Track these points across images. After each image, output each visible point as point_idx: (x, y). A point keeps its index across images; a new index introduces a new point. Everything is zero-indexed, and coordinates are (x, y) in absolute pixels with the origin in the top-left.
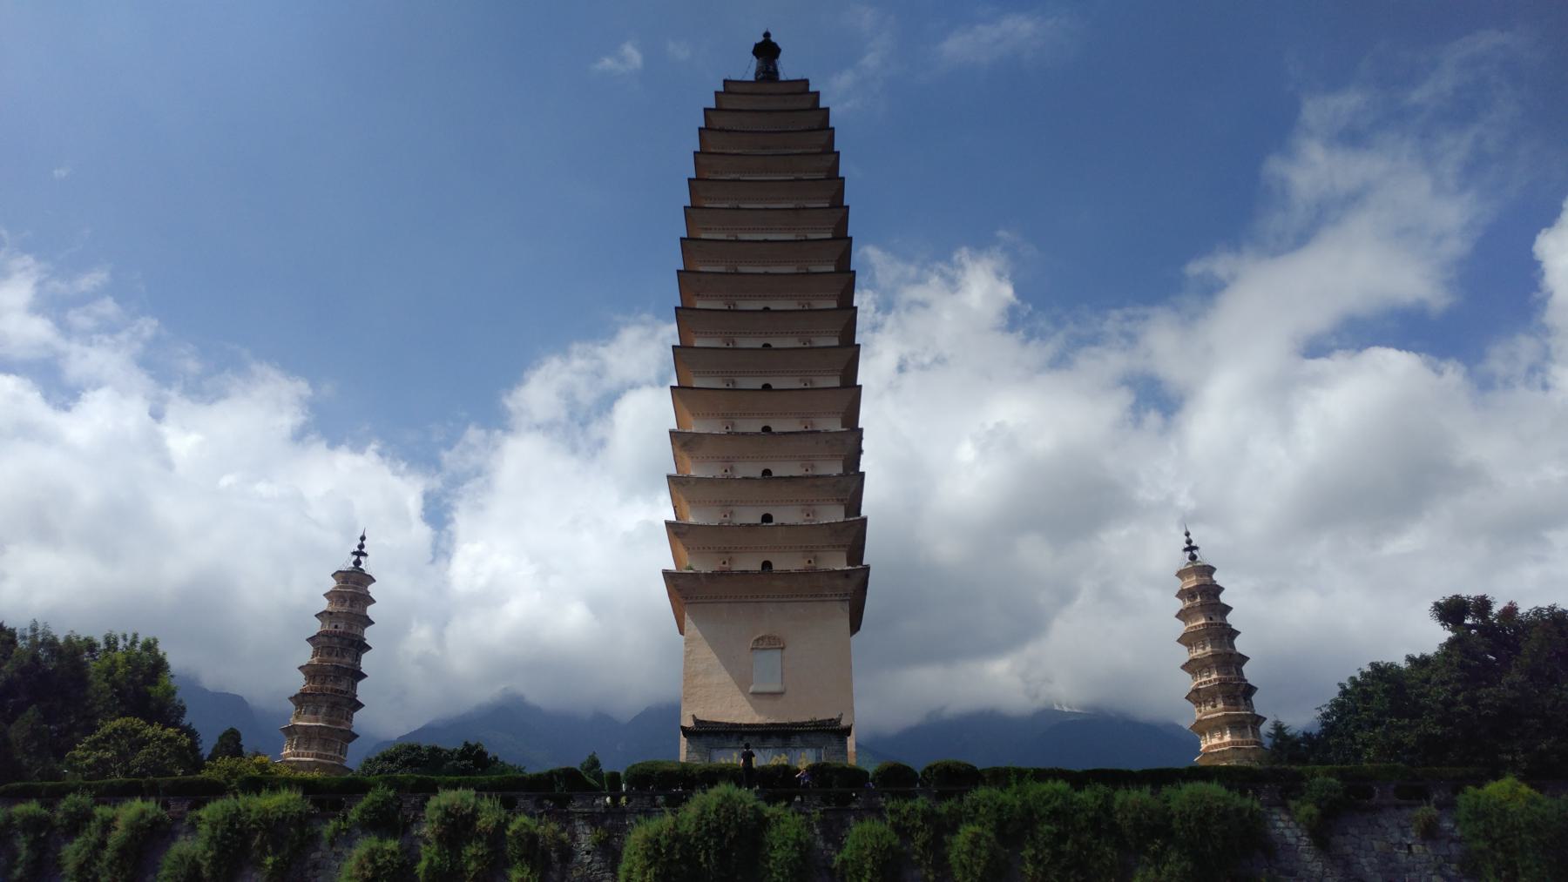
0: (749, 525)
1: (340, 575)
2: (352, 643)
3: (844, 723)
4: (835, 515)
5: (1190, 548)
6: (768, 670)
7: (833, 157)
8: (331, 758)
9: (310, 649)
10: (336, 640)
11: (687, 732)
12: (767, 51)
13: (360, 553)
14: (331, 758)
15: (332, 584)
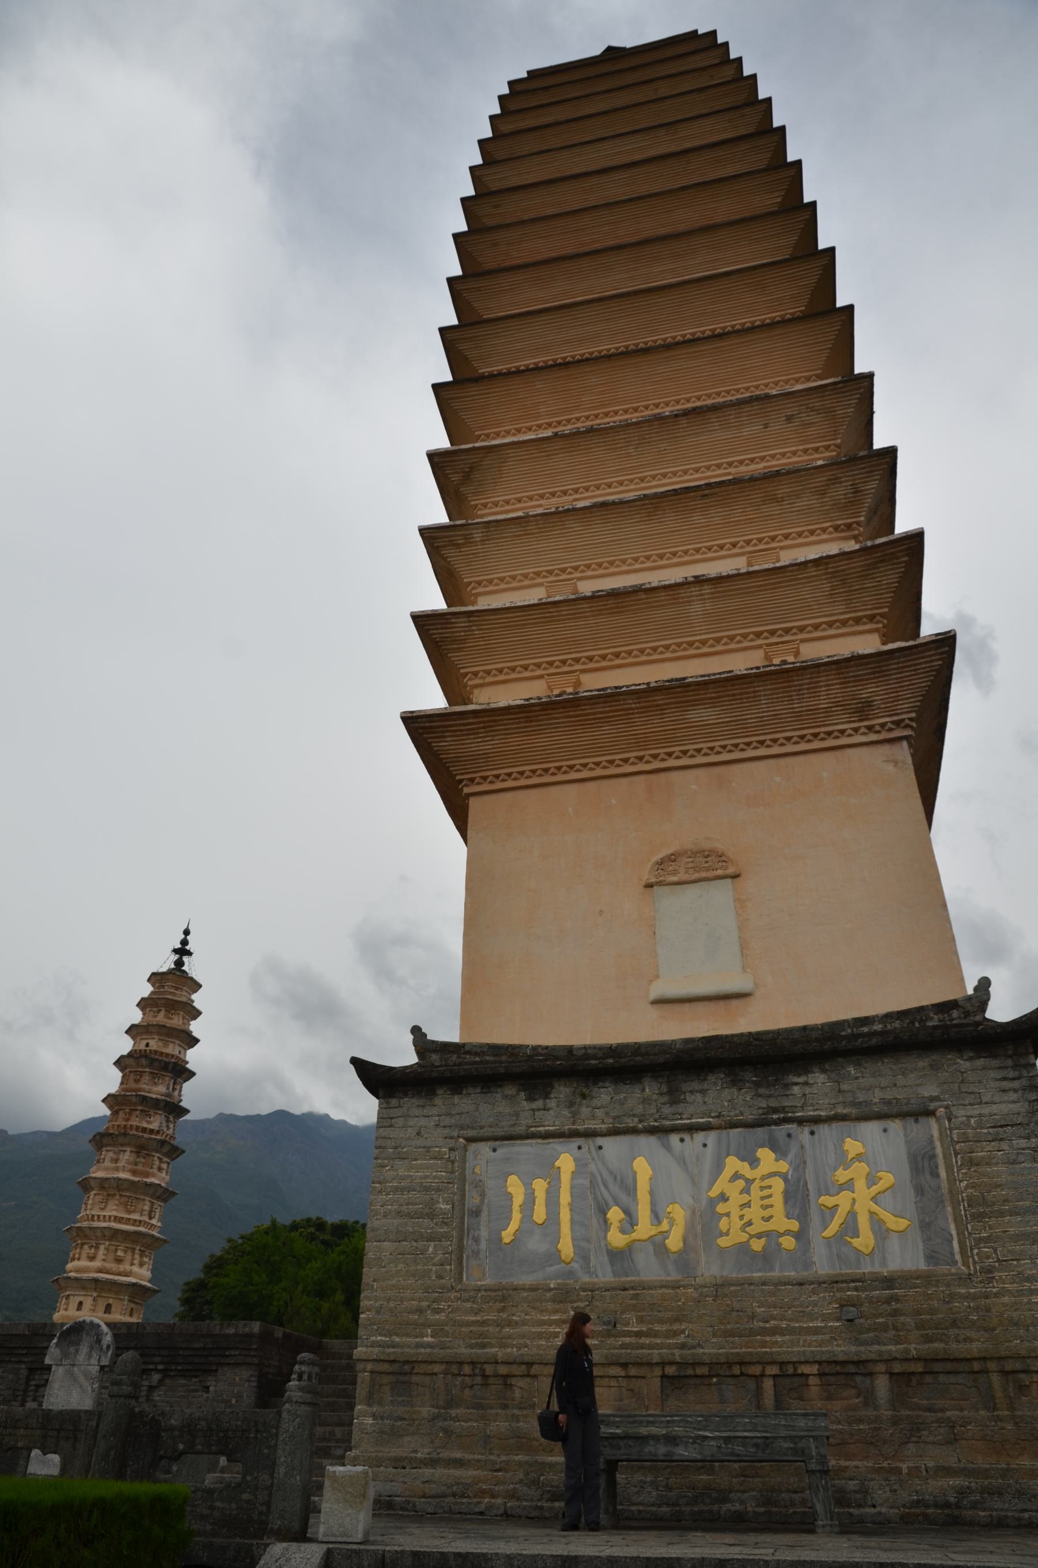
1: (155, 978)
8: (136, 1222)
9: (117, 1075)
10: (144, 1061)
13: (183, 951)
14: (136, 1222)
15: (146, 990)
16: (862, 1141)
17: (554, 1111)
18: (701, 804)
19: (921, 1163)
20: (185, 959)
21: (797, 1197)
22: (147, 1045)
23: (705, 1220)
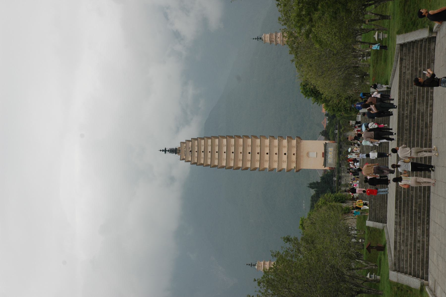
0: (288, 157)
4: (285, 142)
5: (258, 38)
6: (313, 155)
12: (165, 151)
17: (327, 160)
18: (304, 153)
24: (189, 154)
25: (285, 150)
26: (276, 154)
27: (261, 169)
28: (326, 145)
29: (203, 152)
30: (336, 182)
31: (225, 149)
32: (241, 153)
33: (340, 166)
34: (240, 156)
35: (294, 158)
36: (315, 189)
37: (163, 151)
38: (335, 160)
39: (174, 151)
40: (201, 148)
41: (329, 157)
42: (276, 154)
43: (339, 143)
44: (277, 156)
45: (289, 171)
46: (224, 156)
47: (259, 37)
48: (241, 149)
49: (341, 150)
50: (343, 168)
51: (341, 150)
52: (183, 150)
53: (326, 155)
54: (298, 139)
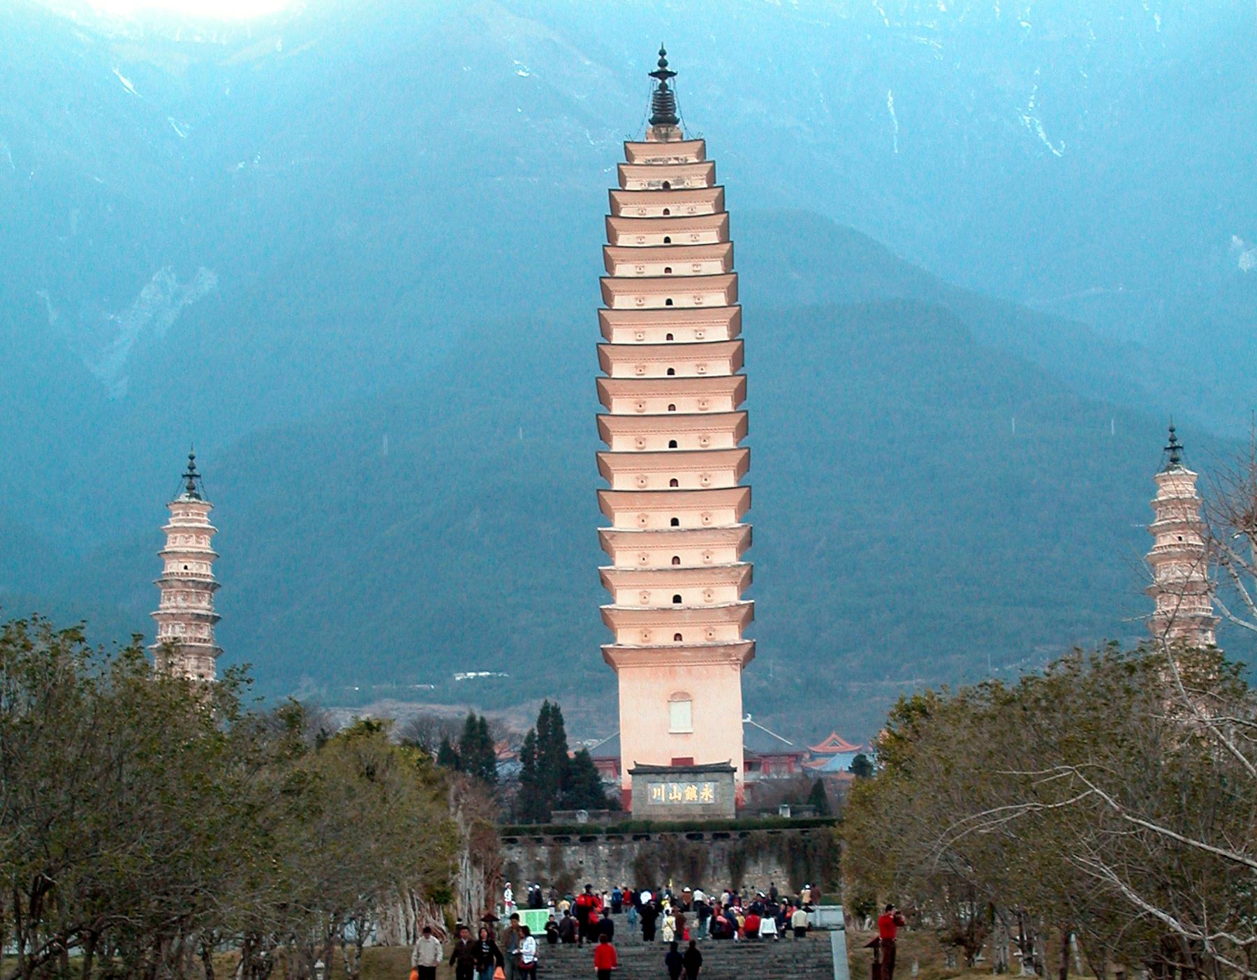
2: (206, 586)
3: (732, 765)
6: (680, 716)
7: (727, 246)
11: (630, 772)
12: (663, 74)
16: (707, 785)
18: (683, 679)
19: (716, 789)
20: (194, 480)
21: (698, 793)
22: (186, 568)
23: (684, 795)
24: (658, 177)
25: (693, 597)
26: (676, 560)
27: (606, 496)
28: (725, 769)
29: (667, 240)
30: (570, 823)
31: (683, 335)
32: (672, 407)
33: (636, 838)
34: (657, 406)
35: (663, 637)
36: (537, 733)
37: (663, 63)
38: (662, 812)
39: (664, 113)
40: (685, 229)
41: (675, 787)
42: (676, 560)
43: (733, 826)
44: (668, 564)
45: (605, 618)
46: (656, 336)
47: (1179, 453)
48: (686, 405)
49: (707, 836)
50: (632, 849)
51: (707, 836)
52: (668, 152)
53: (682, 772)
54: (745, 650)
